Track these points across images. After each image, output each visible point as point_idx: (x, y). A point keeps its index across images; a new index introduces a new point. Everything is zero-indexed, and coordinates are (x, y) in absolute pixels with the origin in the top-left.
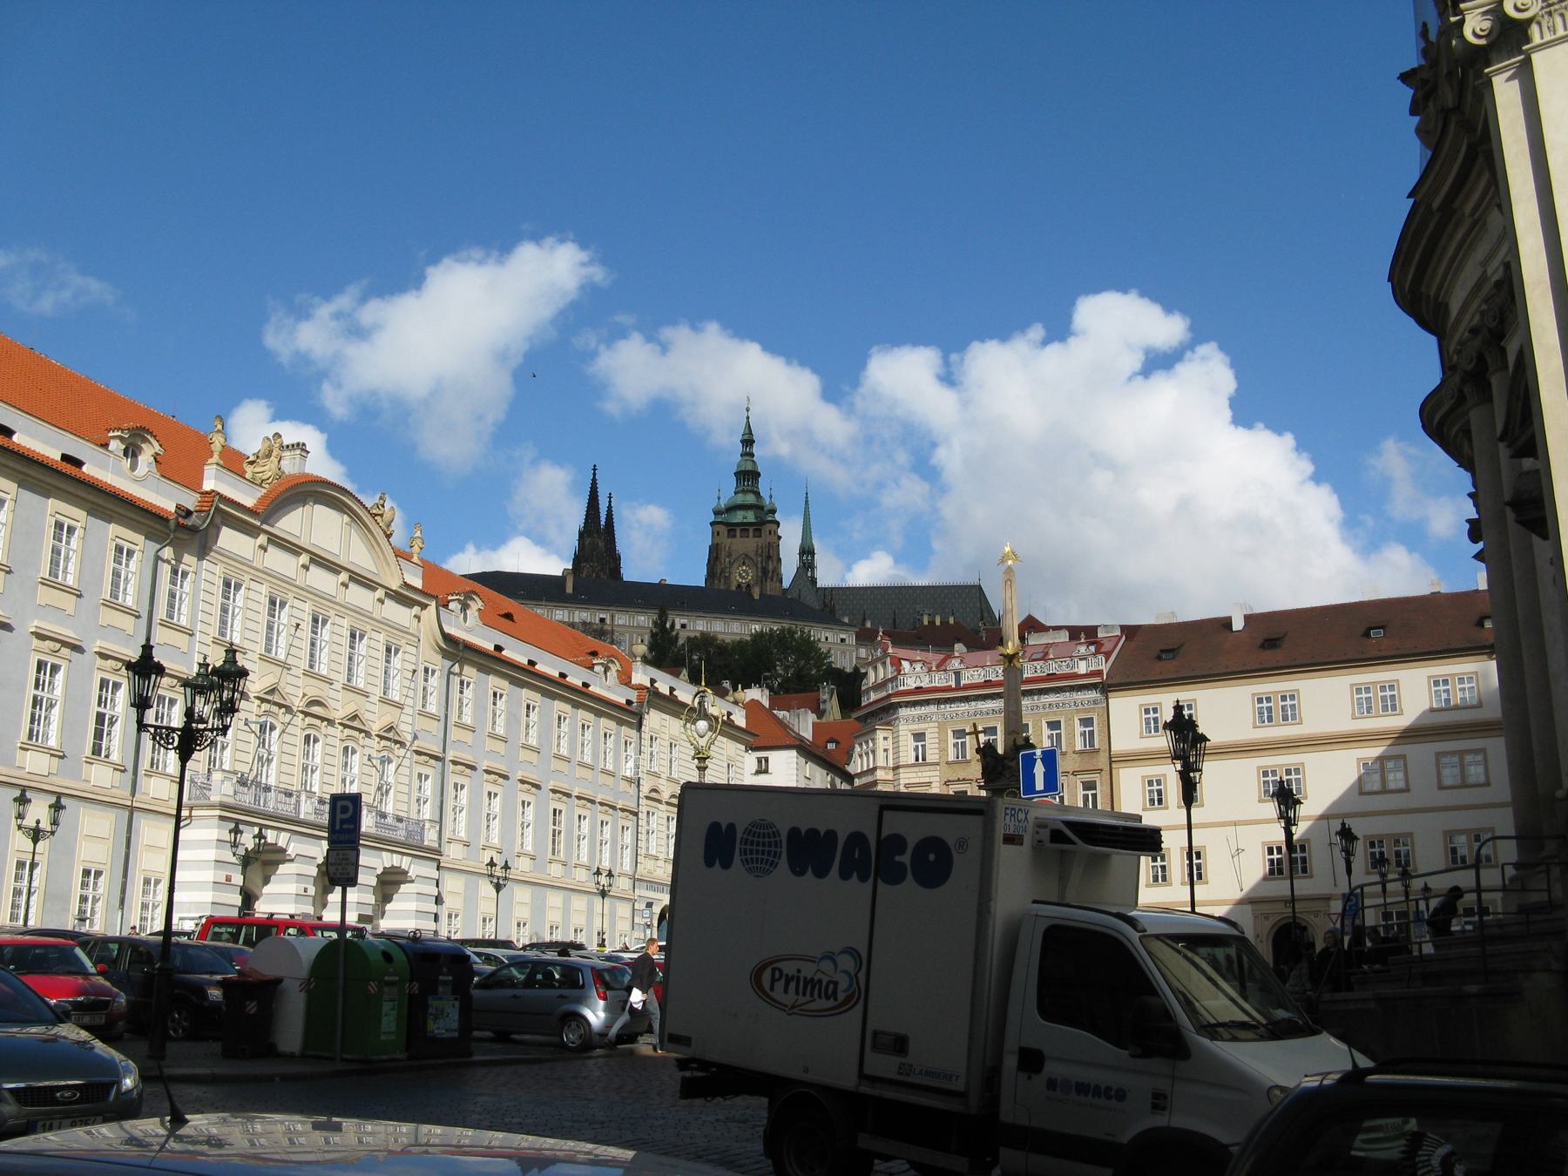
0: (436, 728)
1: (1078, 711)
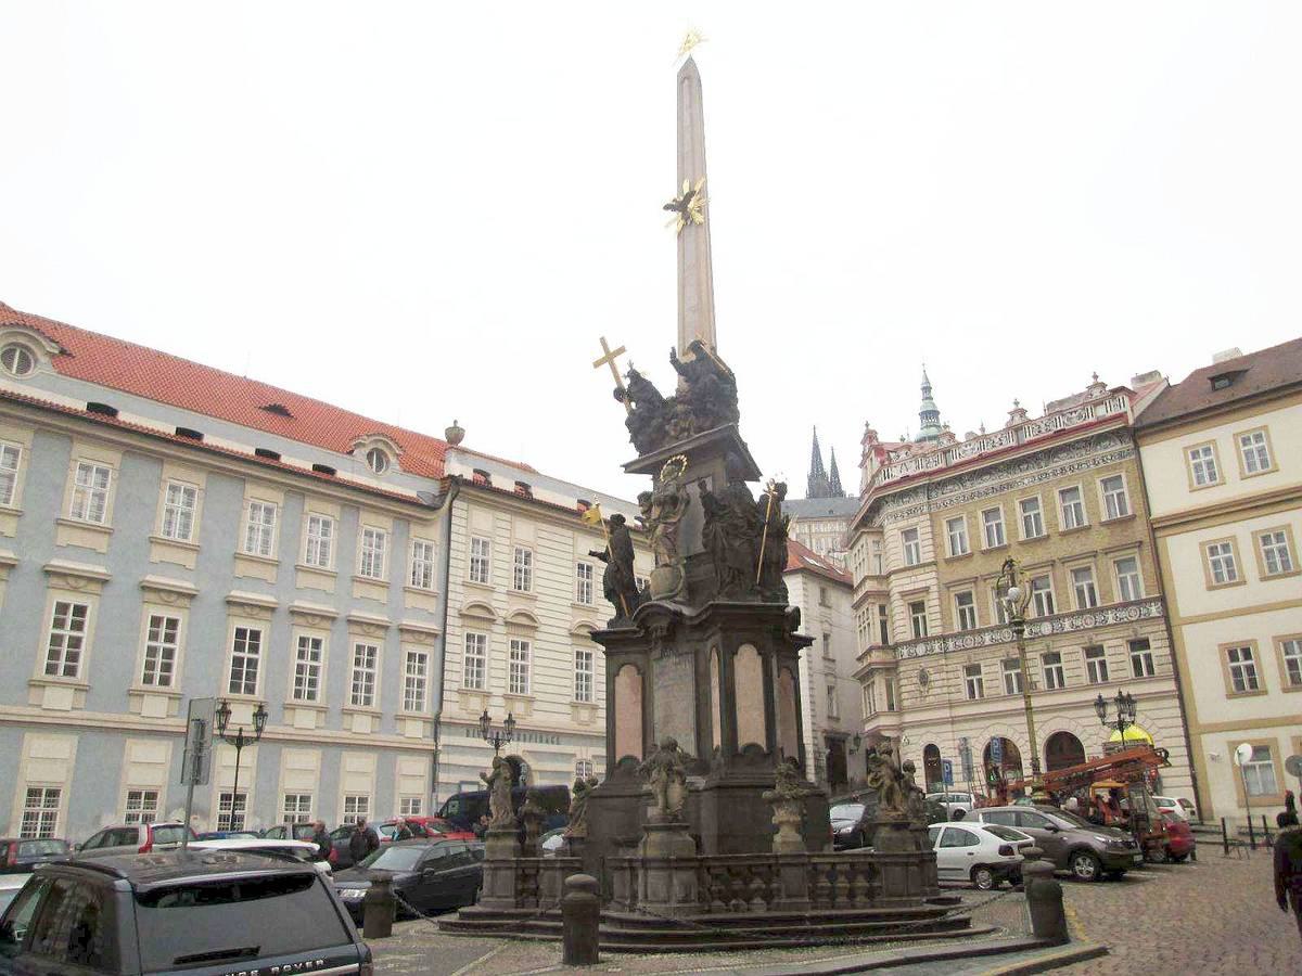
1: (1099, 471)
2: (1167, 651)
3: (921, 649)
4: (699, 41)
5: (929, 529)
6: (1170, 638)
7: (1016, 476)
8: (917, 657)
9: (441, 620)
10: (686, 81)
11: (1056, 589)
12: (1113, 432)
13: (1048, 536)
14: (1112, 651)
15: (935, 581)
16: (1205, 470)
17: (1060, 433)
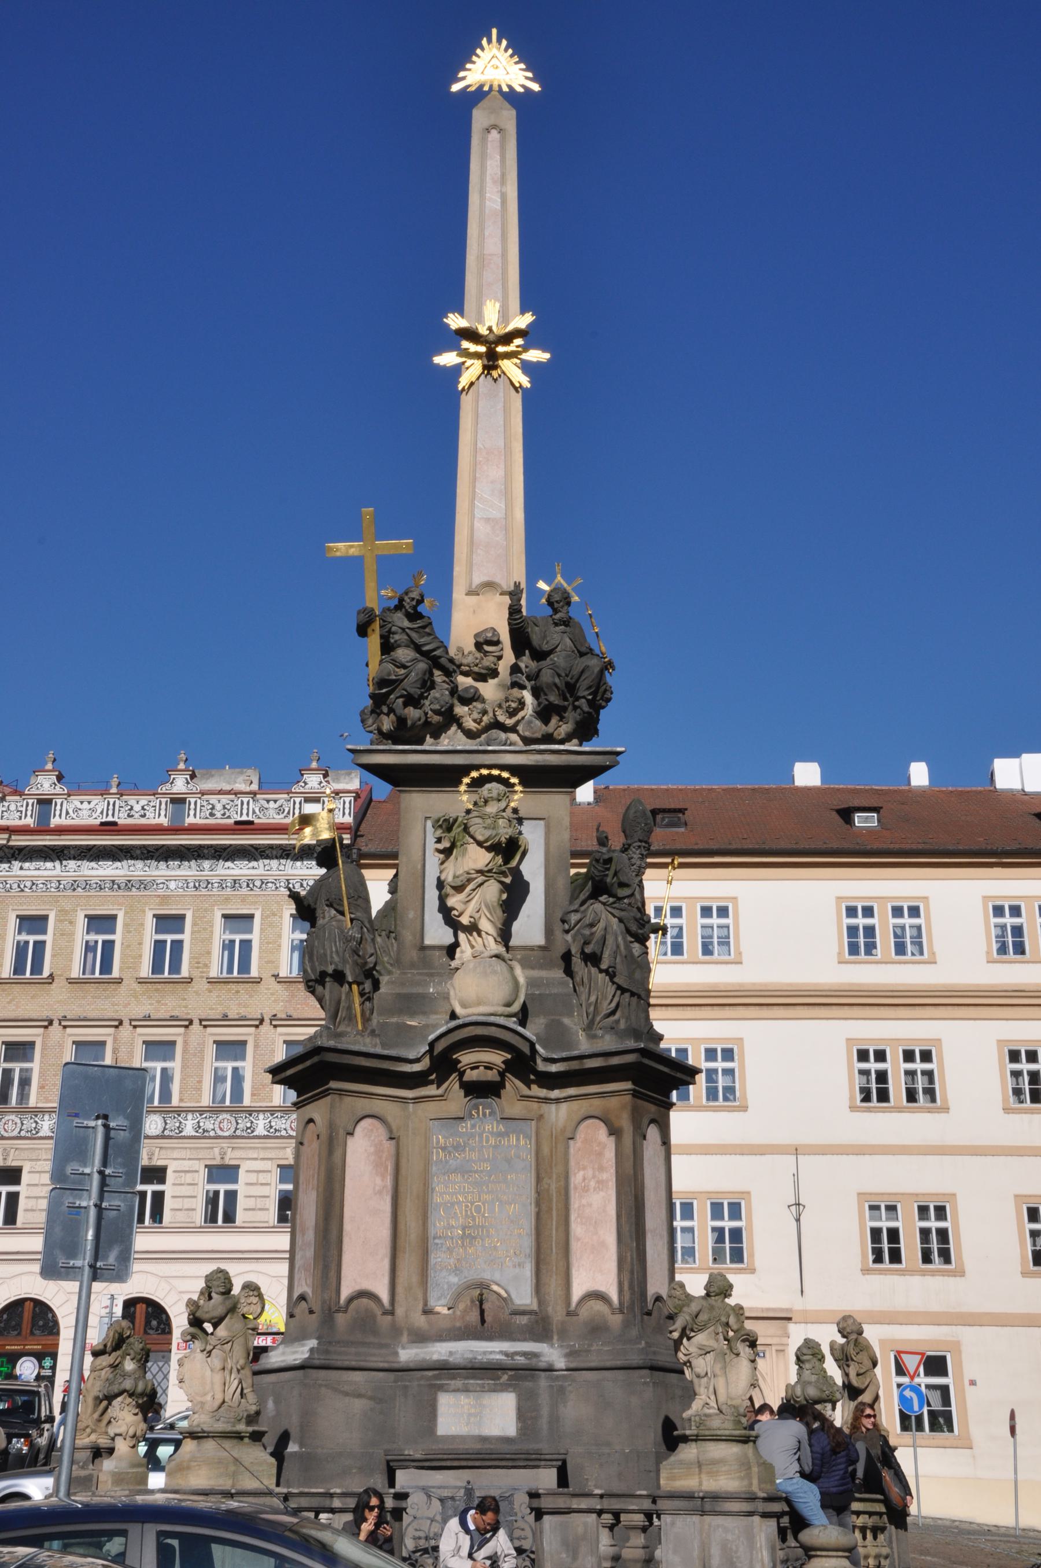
7: (156, 873)
10: (494, 134)
11: (184, 1067)
13: (190, 980)
14: (253, 1178)
17: (244, 826)
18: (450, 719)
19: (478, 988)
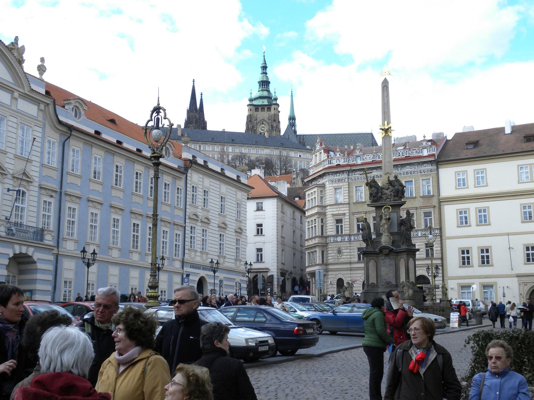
0: (56, 175)
1: (422, 176)
2: (440, 249)
3: (339, 239)
4: (389, 74)
5: (347, 189)
6: (442, 244)
8: (337, 242)
9: (183, 220)
12: (429, 161)
15: (348, 211)
16: (461, 183)
17: (407, 158)
18: (381, 197)
19: (385, 240)
